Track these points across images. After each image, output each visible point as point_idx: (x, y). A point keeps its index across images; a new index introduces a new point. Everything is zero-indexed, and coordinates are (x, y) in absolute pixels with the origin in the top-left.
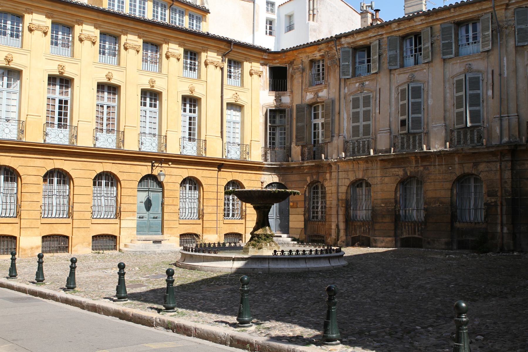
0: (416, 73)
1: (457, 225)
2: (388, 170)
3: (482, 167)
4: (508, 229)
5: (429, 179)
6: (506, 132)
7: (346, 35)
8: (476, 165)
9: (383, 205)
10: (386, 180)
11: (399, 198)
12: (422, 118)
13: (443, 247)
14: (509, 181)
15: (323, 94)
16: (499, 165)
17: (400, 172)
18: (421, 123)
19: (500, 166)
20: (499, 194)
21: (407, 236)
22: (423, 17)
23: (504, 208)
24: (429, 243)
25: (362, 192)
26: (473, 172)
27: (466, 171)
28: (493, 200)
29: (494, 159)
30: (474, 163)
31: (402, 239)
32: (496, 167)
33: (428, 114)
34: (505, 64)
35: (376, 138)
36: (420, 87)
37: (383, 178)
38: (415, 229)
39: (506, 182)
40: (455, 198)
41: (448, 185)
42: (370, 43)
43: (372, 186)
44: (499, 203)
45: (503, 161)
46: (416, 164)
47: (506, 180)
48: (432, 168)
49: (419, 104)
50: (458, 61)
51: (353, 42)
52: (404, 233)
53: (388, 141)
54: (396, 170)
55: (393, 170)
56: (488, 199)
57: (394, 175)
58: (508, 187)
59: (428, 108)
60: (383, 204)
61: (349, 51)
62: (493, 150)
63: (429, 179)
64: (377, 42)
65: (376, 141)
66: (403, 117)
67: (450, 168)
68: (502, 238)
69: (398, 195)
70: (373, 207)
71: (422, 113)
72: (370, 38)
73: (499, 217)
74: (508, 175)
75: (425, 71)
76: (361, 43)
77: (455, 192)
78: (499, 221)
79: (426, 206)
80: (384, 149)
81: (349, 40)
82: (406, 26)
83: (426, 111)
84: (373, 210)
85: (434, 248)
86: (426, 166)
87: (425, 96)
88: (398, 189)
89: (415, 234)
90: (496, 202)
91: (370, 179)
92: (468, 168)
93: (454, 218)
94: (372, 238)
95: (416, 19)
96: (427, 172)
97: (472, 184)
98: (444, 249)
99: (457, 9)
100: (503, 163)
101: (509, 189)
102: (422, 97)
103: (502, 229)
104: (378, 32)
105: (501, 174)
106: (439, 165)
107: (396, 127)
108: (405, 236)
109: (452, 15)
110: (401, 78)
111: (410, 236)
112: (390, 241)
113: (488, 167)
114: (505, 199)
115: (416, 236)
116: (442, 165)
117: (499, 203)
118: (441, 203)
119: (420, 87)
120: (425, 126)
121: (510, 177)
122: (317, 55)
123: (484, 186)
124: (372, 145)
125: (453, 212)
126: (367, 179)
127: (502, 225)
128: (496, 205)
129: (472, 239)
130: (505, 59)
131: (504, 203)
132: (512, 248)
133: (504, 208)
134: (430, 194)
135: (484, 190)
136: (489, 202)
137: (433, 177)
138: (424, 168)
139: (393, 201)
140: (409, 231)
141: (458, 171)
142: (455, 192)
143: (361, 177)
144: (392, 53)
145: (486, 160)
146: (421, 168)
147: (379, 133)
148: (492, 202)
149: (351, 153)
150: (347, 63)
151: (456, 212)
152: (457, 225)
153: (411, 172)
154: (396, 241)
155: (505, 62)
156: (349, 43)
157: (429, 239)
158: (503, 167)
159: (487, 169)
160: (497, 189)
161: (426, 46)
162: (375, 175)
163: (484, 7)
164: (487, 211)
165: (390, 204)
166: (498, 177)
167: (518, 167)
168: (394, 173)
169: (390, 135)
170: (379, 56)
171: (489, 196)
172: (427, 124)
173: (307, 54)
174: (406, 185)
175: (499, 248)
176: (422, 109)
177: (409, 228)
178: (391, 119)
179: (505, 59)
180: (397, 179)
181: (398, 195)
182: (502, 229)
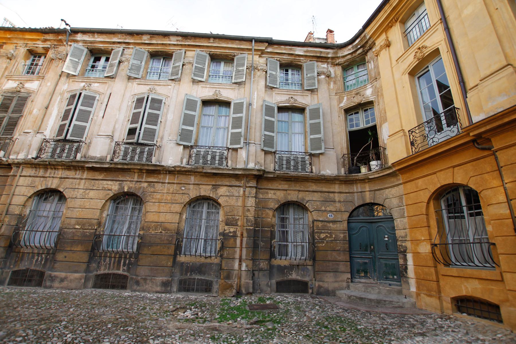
0: (160, 87)
1: (182, 259)
2: (97, 182)
3: (222, 191)
4: (247, 266)
5: (153, 198)
6: (252, 158)
7: (85, 32)
8: (215, 187)
9: (77, 227)
10: (92, 194)
11: (104, 219)
12: (157, 131)
13: (159, 289)
14: (252, 210)
15: (32, 85)
16: (242, 190)
17: (114, 187)
18: (154, 136)
19: (244, 191)
20: (239, 223)
21: (107, 271)
22: (180, 38)
23: (245, 239)
24: (137, 283)
25: (49, 207)
26: (211, 196)
27: (203, 194)
28: (232, 230)
29: (237, 183)
30: (213, 185)
31: (97, 276)
32: (239, 193)
33: (164, 128)
34: (256, 98)
35: (90, 143)
36: (161, 101)
37: (88, 191)
38: (119, 262)
39: (248, 210)
40: (183, 224)
41: (178, 208)
42: (112, 50)
43: (68, 200)
44: (239, 234)
45: (247, 187)
46: (138, 178)
47: (249, 208)
48: (159, 186)
49: (157, 116)
50: (208, 86)
51: (91, 42)
52: (103, 268)
53: (107, 147)
54: (109, 183)
55: (105, 182)
56: (226, 227)
57: (104, 189)
58: (251, 215)
59: (166, 121)
60: (79, 225)
61: (83, 51)
62: (240, 173)
63: (153, 198)
64: (121, 49)
65: (89, 146)
66: (134, 126)
67: (183, 188)
68: (240, 278)
69: (104, 215)
70: (61, 229)
71: (158, 125)
72: (114, 43)
73: (238, 250)
74: (251, 202)
75: (170, 87)
76: (101, 46)
77: (184, 217)
78: (237, 256)
79: (142, 233)
80: (98, 156)
81: (87, 38)
82: (159, 42)
83: (163, 124)
84: (61, 234)
85: (144, 291)
86: (152, 182)
87: (165, 110)
88: (107, 207)
89: (119, 269)
90: (235, 232)
91: (66, 190)
92: (205, 190)
93: (178, 248)
94: (48, 273)
95: (172, 38)
96: (152, 190)
97: (205, 210)
98: (159, 292)
99: (217, 40)
100: (247, 189)
101: (252, 219)
102: (162, 110)
103: (240, 265)
104: (125, 39)
105: (244, 201)
106: (169, 183)
107: (121, 135)
108: (102, 271)
109: (210, 45)
110: (139, 89)
111: (110, 272)
112: (76, 279)
113: (229, 192)
114: (247, 229)
115: (120, 272)
116: (174, 183)
117: (239, 234)
118: (165, 229)
119: (161, 101)
120: (159, 140)
121: (254, 205)
122: (40, 45)
123: (221, 212)
124: (83, 150)
125: (177, 243)
126: (62, 190)
127: (240, 261)
128: (235, 236)
129: (200, 278)
130: (256, 93)
131: (245, 234)
132: (251, 290)
133: (245, 239)
134: (151, 217)
135: (221, 217)
136: (227, 231)
137: (158, 196)
138: (149, 185)
139: (95, 221)
140: (110, 264)
141: (193, 193)
142: (184, 217)
143: (54, 187)
144: (135, 62)
145: (228, 184)
146: (145, 185)
147: (96, 138)
148: (230, 232)
149: (50, 154)
150: (77, 60)
151: (182, 241)
152: (182, 259)
153: (129, 188)
154: (87, 279)
155: (256, 95)
156: (85, 42)
157: (139, 278)
158: (246, 193)
159: (228, 194)
160: (238, 217)
161: (177, 65)
162: (77, 187)
163: (242, 47)
164: (223, 243)
165: (89, 226)
166: (240, 203)
167: (261, 196)
168: (106, 186)
169: (111, 142)
170: (120, 62)
171: (227, 224)
172: (162, 138)
173: (26, 42)
174: (118, 204)
175: (234, 291)
176: (159, 122)
177: (110, 261)
178: (117, 126)
179: (256, 93)
180: (108, 194)
181: (104, 215)
182: (240, 265)
